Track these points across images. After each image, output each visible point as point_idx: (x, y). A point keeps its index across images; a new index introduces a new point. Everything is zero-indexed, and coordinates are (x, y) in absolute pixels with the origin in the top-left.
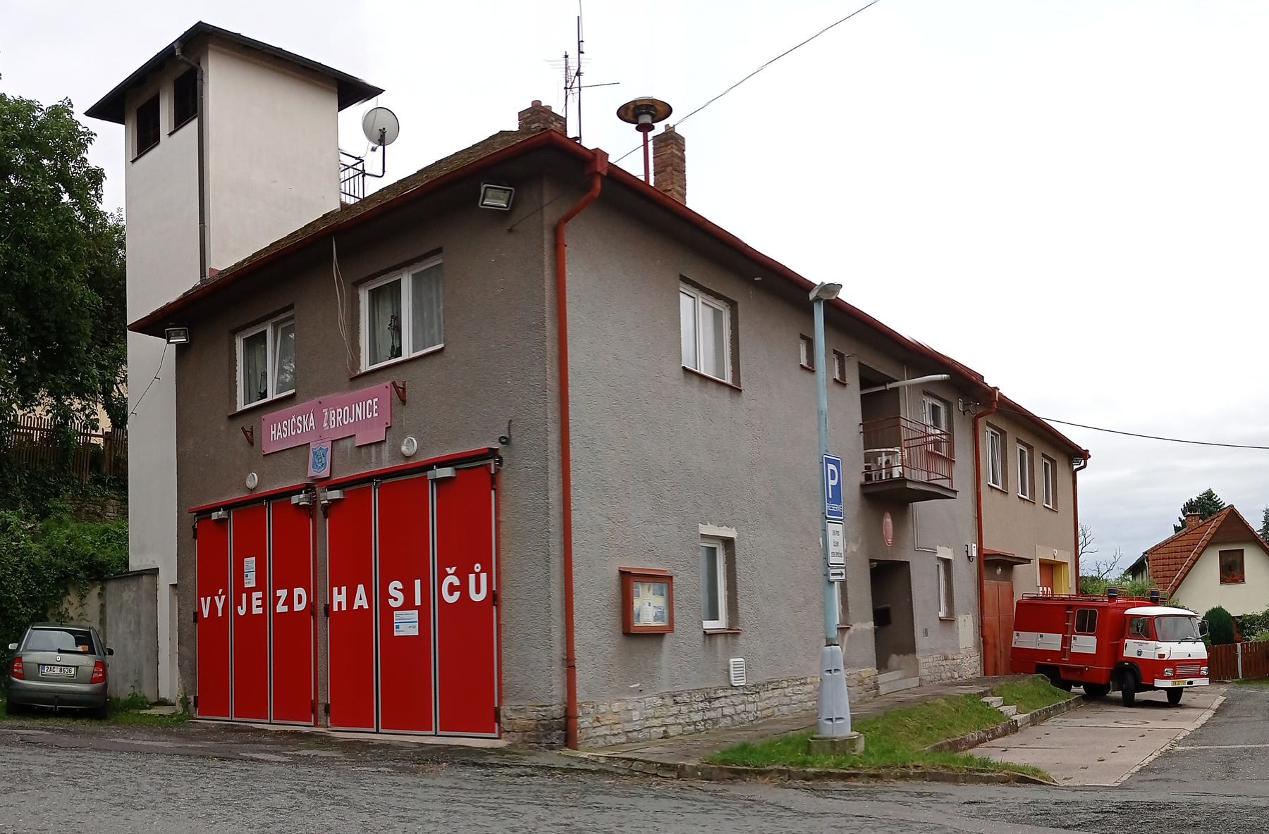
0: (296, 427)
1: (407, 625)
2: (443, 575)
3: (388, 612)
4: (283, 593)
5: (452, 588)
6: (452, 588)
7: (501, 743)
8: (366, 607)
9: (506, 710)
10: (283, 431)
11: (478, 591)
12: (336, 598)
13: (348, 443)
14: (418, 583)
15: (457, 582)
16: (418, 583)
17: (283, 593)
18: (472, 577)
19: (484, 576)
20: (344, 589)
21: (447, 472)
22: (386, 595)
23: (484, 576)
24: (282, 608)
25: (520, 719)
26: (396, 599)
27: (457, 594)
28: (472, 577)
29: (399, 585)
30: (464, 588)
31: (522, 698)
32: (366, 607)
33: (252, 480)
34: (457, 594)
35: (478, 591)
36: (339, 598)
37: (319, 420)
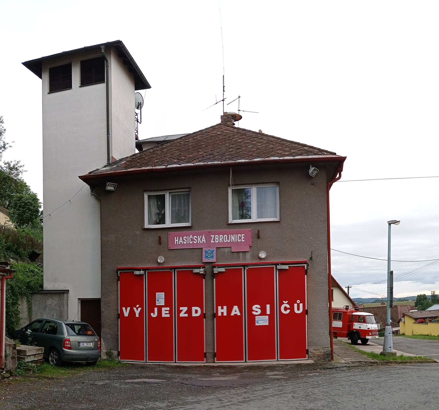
0: (192, 240)
1: (262, 321)
2: (281, 304)
3: (252, 318)
4: (185, 309)
5: (286, 309)
6: (286, 309)
7: (311, 361)
8: (239, 314)
9: (311, 350)
10: (183, 241)
11: (298, 309)
12: (220, 310)
13: (226, 250)
14: (268, 306)
15: (288, 306)
16: (268, 306)
17: (185, 309)
18: (296, 305)
19: (301, 305)
20: (225, 307)
21: (286, 267)
22: (250, 310)
23: (301, 305)
24: (182, 315)
25: (317, 353)
26: (257, 312)
27: (288, 311)
28: (296, 305)
29: (259, 306)
30: (292, 308)
31: (317, 346)
32: (239, 314)
33: (161, 260)
34: (288, 311)
35: (298, 309)
36: (222, 311)
37: (208, 239)
